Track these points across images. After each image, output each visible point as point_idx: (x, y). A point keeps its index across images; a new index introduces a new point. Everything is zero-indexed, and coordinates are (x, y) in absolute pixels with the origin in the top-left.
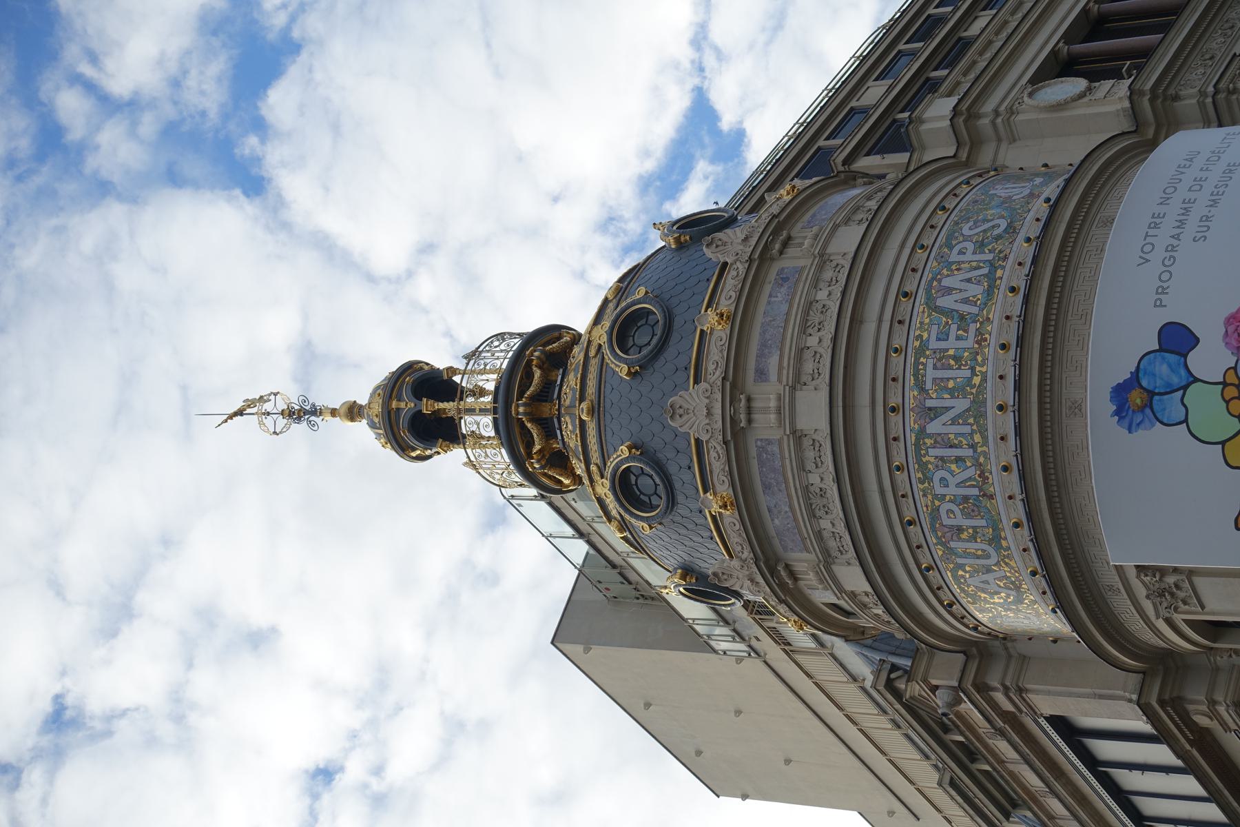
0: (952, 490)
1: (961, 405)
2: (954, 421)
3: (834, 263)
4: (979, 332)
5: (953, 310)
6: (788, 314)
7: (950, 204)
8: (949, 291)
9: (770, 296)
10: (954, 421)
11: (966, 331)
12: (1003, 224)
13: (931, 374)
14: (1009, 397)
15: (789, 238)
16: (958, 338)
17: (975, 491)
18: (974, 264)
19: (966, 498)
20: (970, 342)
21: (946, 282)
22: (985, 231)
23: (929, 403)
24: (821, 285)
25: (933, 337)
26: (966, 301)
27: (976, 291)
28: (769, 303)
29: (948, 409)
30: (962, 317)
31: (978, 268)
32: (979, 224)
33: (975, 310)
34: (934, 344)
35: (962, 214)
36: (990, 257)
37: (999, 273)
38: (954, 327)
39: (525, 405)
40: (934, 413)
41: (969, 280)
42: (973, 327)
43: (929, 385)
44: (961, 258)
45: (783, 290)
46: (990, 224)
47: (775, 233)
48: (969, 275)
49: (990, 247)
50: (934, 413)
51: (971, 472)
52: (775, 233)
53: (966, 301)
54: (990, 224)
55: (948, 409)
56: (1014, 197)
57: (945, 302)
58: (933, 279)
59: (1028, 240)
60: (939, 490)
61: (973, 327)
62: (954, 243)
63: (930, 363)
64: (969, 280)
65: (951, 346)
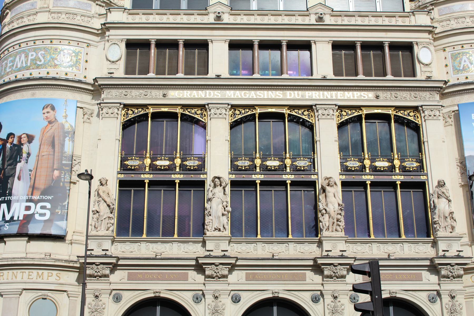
4: (9, 72)
5: (15, 61)
9: (28, 3)
13: (4, 64)
14: (51, 75)
20: (8, 70)
27: (19, 66)
28: (26, 4)
30: (13, 65)
32: (43, 55)
35: (50, 48)
36: (29, 64)
38: (11, 64)
41: (22, 62)
42: (11, 69)
45: (30, 6)
53: (17, 65)
59: (31, 74)
61: (11, 69)
64: (22, 62)
65: (9, 65)
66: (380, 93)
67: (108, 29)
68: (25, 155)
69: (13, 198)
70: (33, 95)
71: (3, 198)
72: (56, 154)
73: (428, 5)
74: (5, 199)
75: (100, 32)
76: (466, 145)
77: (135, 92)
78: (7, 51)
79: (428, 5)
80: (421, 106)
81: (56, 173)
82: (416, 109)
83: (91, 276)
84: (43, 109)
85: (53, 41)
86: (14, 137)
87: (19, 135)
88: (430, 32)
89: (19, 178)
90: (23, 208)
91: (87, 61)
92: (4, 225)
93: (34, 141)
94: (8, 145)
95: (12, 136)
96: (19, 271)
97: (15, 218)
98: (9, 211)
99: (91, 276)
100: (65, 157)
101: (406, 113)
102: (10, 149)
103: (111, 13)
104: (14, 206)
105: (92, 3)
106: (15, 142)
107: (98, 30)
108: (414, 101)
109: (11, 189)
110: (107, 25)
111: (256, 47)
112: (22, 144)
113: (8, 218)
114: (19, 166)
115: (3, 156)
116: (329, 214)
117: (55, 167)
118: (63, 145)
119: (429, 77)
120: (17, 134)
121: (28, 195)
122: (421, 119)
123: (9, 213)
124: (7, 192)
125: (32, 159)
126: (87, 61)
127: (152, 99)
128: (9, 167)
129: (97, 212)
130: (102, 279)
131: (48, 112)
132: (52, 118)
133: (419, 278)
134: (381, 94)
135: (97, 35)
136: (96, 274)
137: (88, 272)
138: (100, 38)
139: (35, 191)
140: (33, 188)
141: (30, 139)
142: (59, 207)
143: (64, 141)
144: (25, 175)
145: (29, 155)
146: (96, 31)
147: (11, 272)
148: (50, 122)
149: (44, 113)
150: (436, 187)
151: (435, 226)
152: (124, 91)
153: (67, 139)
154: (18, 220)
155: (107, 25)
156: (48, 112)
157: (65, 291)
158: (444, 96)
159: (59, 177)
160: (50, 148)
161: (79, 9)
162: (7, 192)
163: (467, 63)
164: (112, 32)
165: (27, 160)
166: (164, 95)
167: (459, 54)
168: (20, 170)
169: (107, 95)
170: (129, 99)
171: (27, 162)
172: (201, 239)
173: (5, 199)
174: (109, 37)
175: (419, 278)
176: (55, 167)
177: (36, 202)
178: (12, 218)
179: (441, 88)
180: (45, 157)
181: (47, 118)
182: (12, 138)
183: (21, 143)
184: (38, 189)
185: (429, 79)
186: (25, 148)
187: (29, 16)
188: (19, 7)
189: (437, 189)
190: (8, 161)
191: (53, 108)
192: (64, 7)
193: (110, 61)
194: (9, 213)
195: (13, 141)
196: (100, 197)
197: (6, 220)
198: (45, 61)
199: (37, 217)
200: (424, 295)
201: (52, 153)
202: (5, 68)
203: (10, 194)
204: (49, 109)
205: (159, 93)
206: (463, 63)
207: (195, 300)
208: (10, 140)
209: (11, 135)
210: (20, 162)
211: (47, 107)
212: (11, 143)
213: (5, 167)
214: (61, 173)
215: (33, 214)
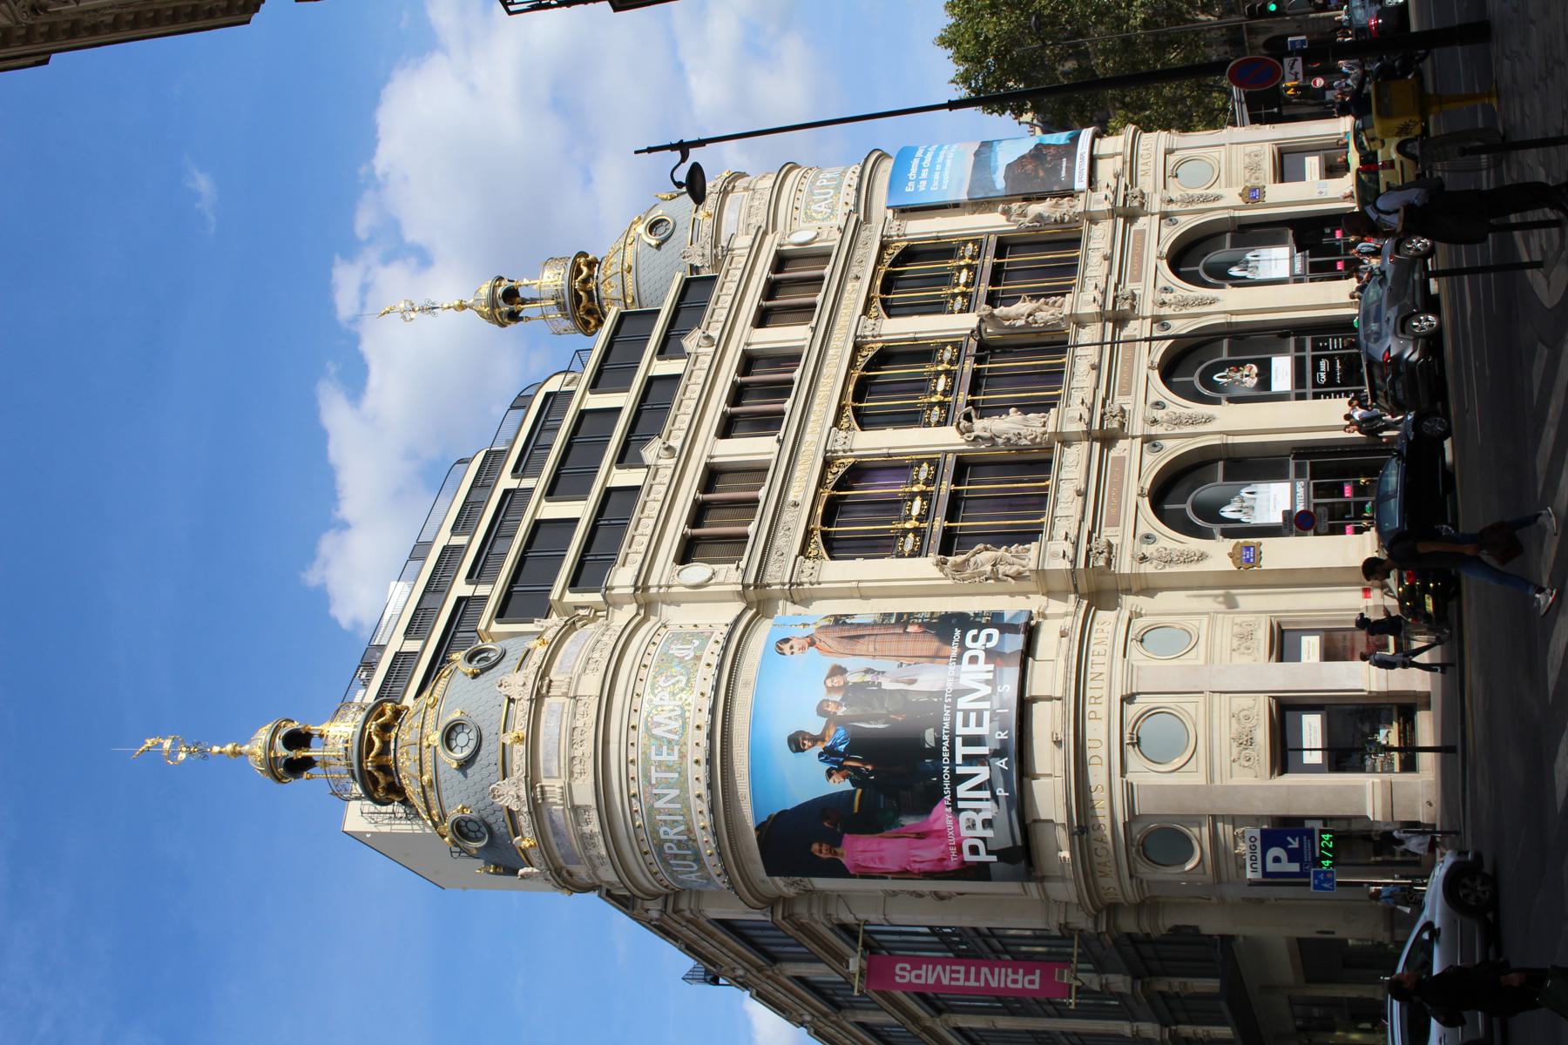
0: (671, 836)
1: (674, 793)
2: (669, 802)
3: (583, 702)
6: (560, 734)
7: (647, 661)
8: (659, 724)
9: (546, 722)
10: (669, 802)
11: (673, 750)
12: (684, 679)
13: (654, 775)
15: (551, 681)
16: (668, 754)
17: (685, 837)
18: (671, 708)
19: (679, 841)
20: (675, 757)
21: (656, 719)
22: (674, 684)
23: (655, 791)
24: (578, 716)
25: (653, 752)
26: (670, 731)
27: (676, 725)
29: (666, 795)
30: (669, 742)
31: (673, 710)
33: (676, 737)
34: (654, 758)
37: (687, 714)
38: (665, 748)
39: (371, 762)
40: (659, 797)
41: (670, 718)
42: (676, 748)
43: (654, 782)
44: (661, 703)
45: (554, 718)
46: (676, 679)
47: (542, 678)
48: (670, 715)
49: (678, 696)
50: (659, 797)
51: (682, 828)
52: (542, 678)
53: (670, 731)
54: (676, 679)
55: (666, 795)
56: (687, 658)
57: (657, 731)
58: (648, 716)
60: (663, 837)
61: (676, 748)
62: (656, 692)
63: (653, 768)
64: (670, 718)
65: (664, 757)
66: (851, 275)
67: (646, 588)
68: (868, 678)
69: (950, 686)
70: (746, 684)
71: (945, 707)
72: (876, 632)
73: (714, 251)
74: (948, 704)
75: (642, 612)
76: (950, 197)
77: (780, 542)
78: (630, 766)
79: (714, 251)
80: (883, 236)
81: (911, 629)
82: (884, 246)
83: (1109, 561)
84: (783, 654)
85: (644, 662)
86: (828, 701)
87: (825, 690)
88: (765, 233)
89: (913, 682)
90: (973, 667)
91: (696, 626)
92: (1001, 694)
93: (843, 666)
94: (842, 711)
95: (825, 704)
96: (1089, 670)
97: (990, 676)
98: (975, 691)
99: (1109, 561)
100: (883, 620)
101: (887, 257)
102: (851, 706)
103: (613, 588)
104: (966, 681)
105: (575, 634)
106: (837, 697)
107: (637, 614)
108: (872, 244)
109: (931, 694)
110: (640, 584)
111: (697, 531)
112: (846, 683)
113: (987, 690)
114: (887, 685)
115: (859, 721)
116: (1035, 310)
117: (901, 631)
118: (859, 625)
119: (839, 228)
120: (821, 694)
121: (948, 664)
122: (902, 241)
123: (978, 690)
124: (936, 700)
125: (876, 664)
126: (696, 626)
127: (797, 523)
128: (886, 705)
129: (994, 565)
130: (1114, 551)
131: (792, 647)
132: (805, 642)
133: (1120, 461)
134: (854, 271)
135: (645, 619)
136: (1105, 554)
137: (1101, 563)
138: (652, 617)
139: (941, 654)
140: (935, 657)
141: (838, 671)
142: (978, 619)
143: (852, 624)
144: (907, 672)
145: (868, 671)
146: (638, 618)
147: (1089, 684)
148: (812, 644)
149: (792, 653)
150: (1008, 220)
151: (1067, 218)
152: (774, 556)
153: (848, 621)
154: (994, 672)
155: (640, 584)
156: (792, 647)
157: (1130, 620)
158: (867, 219)
159: (920, 625)
160: (861, 640)
161: (586, 641)
162: (936, 700)
163: (823, 204)
164: (653, 581)
165: (879, 672)
166: (796, 505)
167: (806, 213)
168: (897, 681)
169: (778, 573)
170: (791, 549)
171: (883, 672)
172: (1058, 446)
173: (948, 704)
174: (660, 587)
175: (1120, 461)
176: (901, 631)
177: (963, 648)
178: (987, 682)
179: (858, 220)
180: (877, 647)
181: (803, 648)
182: (828, 706)
183: (846, 687)
184: (938, 650)
185: (843, 231)
186: (853, 678)
187: (575, 715)
188: (545, 747)
189: (1013, 218)
190: (874, 709)
191: (786, 641)
192: (577, 659)
193: (711, 579)
194: (978, 690)
195: (835, 702)
196: (968, 560)
197: (990, 692)
198: (681, 674)
199: (989, 645)
200: (1165, 231)
201: (873, 638)
202: (669, 768)
203: (941, 693)
204: (786, 647)
205: (787, 516)
206: (823, 209)
207: (1157, 449)
208: (831, 708)
209: (821, 711)
210: (880, 684)
211: (781, 649)
212: (838, 704)
213: (884, 712)
214: (913, 623)
215: (987, 651)
